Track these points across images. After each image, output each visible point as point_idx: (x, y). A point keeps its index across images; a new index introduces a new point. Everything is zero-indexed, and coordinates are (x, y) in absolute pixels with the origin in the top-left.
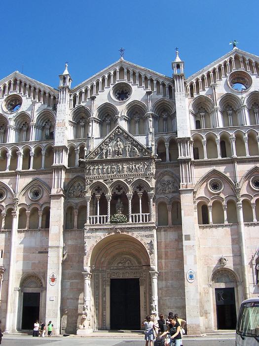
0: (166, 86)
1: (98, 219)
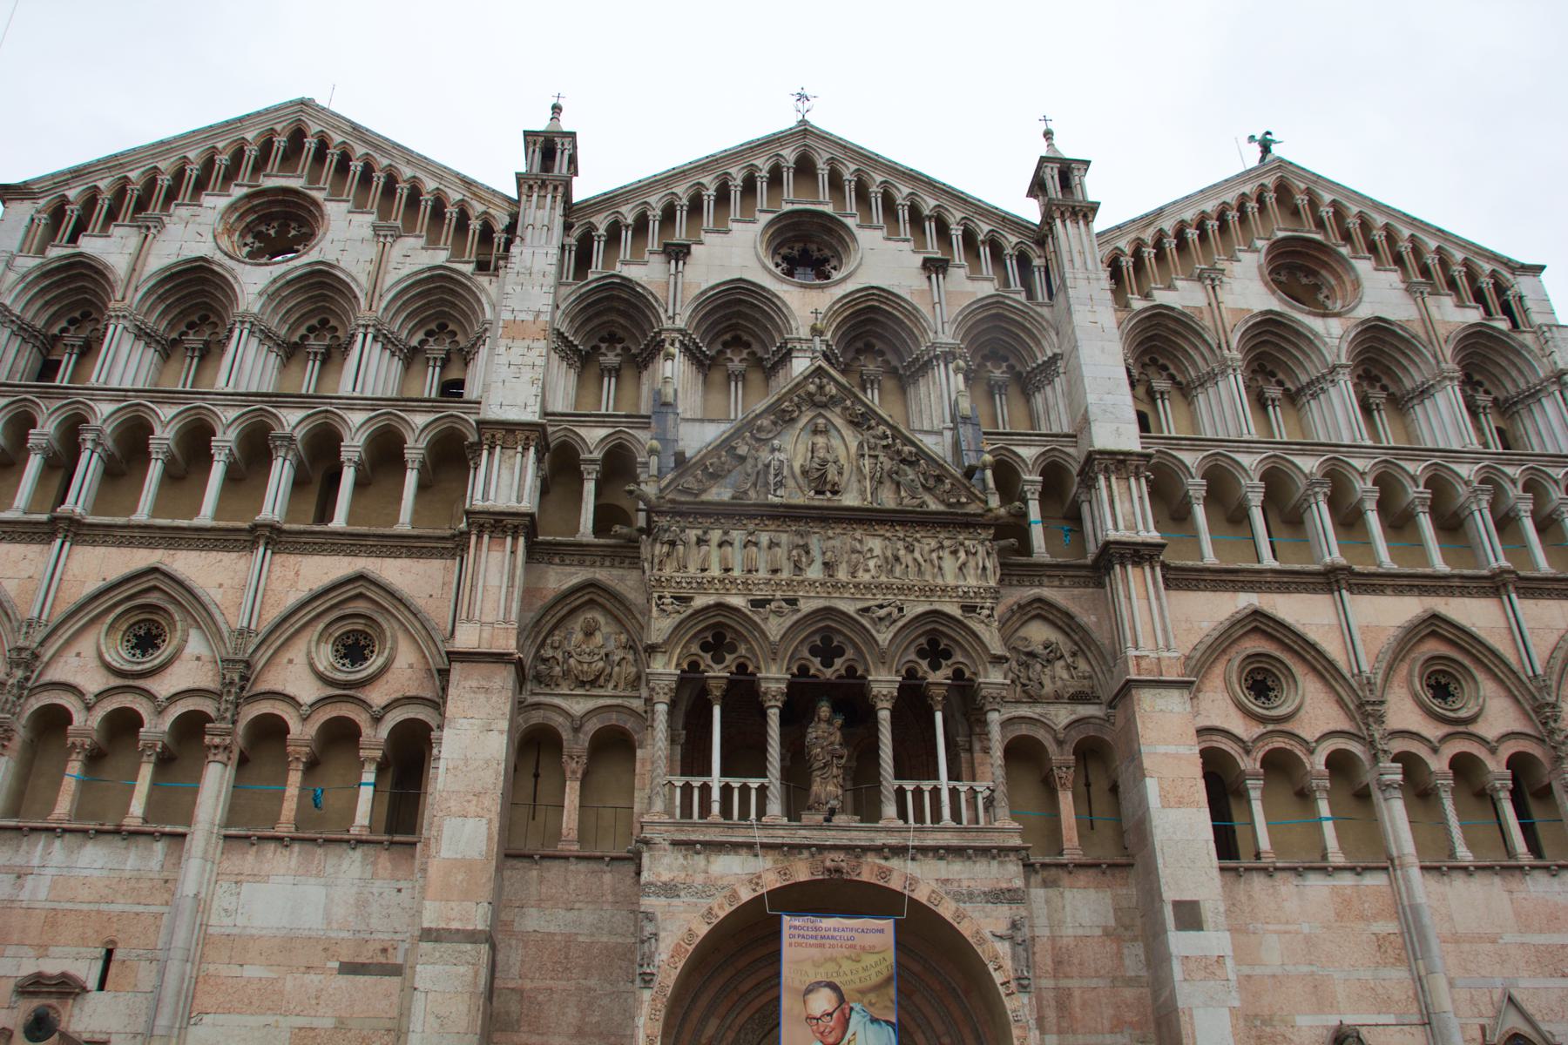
1: (716, 794)
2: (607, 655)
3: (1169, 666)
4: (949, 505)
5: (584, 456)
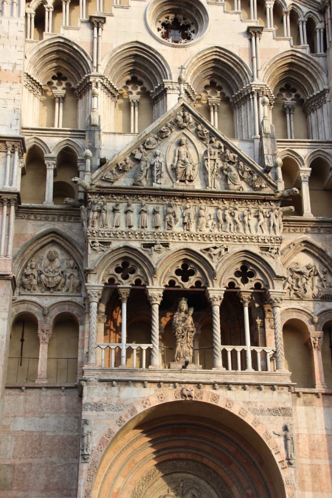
0: (301, 19)
2: (62, 272)
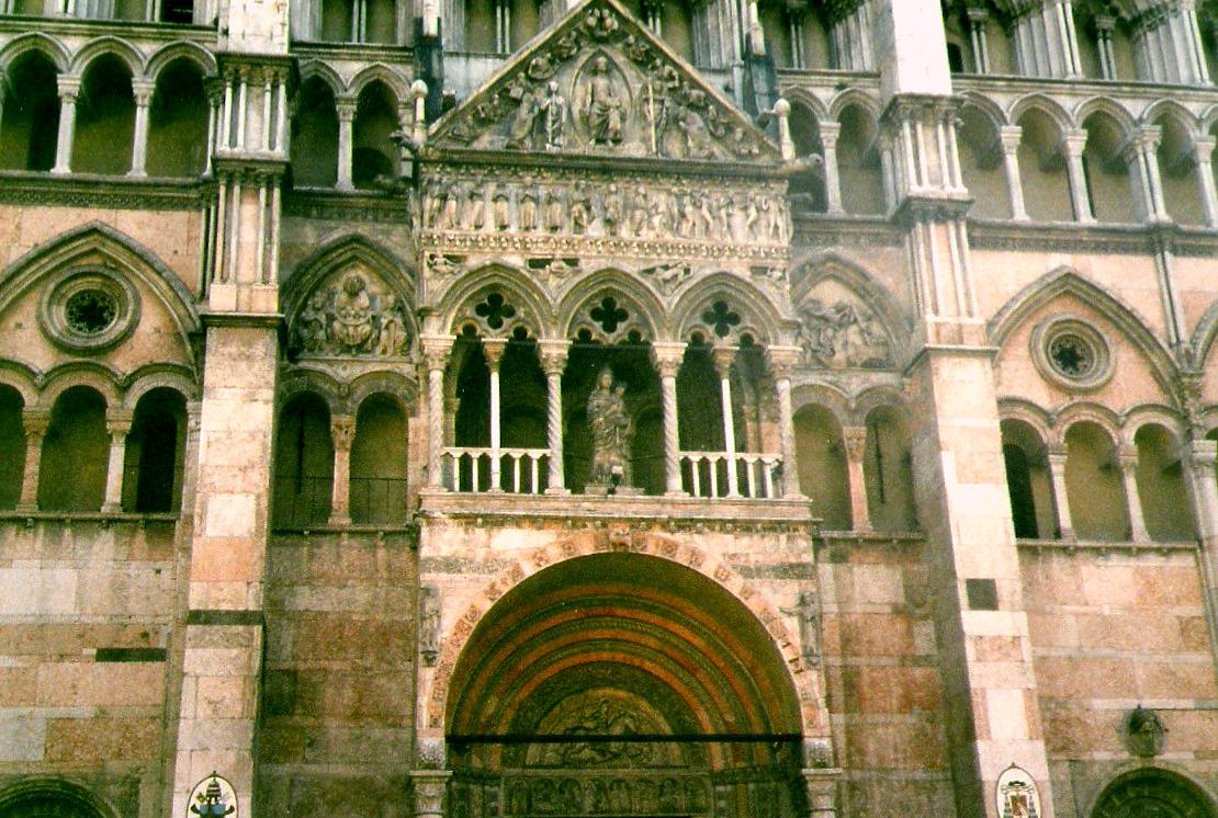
1: (496, 467)
2: (373, 317)
3: (970, 333)
4: (739, 156)
5: (340, 94)
